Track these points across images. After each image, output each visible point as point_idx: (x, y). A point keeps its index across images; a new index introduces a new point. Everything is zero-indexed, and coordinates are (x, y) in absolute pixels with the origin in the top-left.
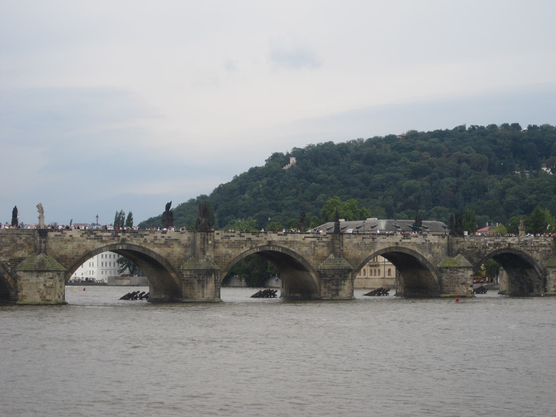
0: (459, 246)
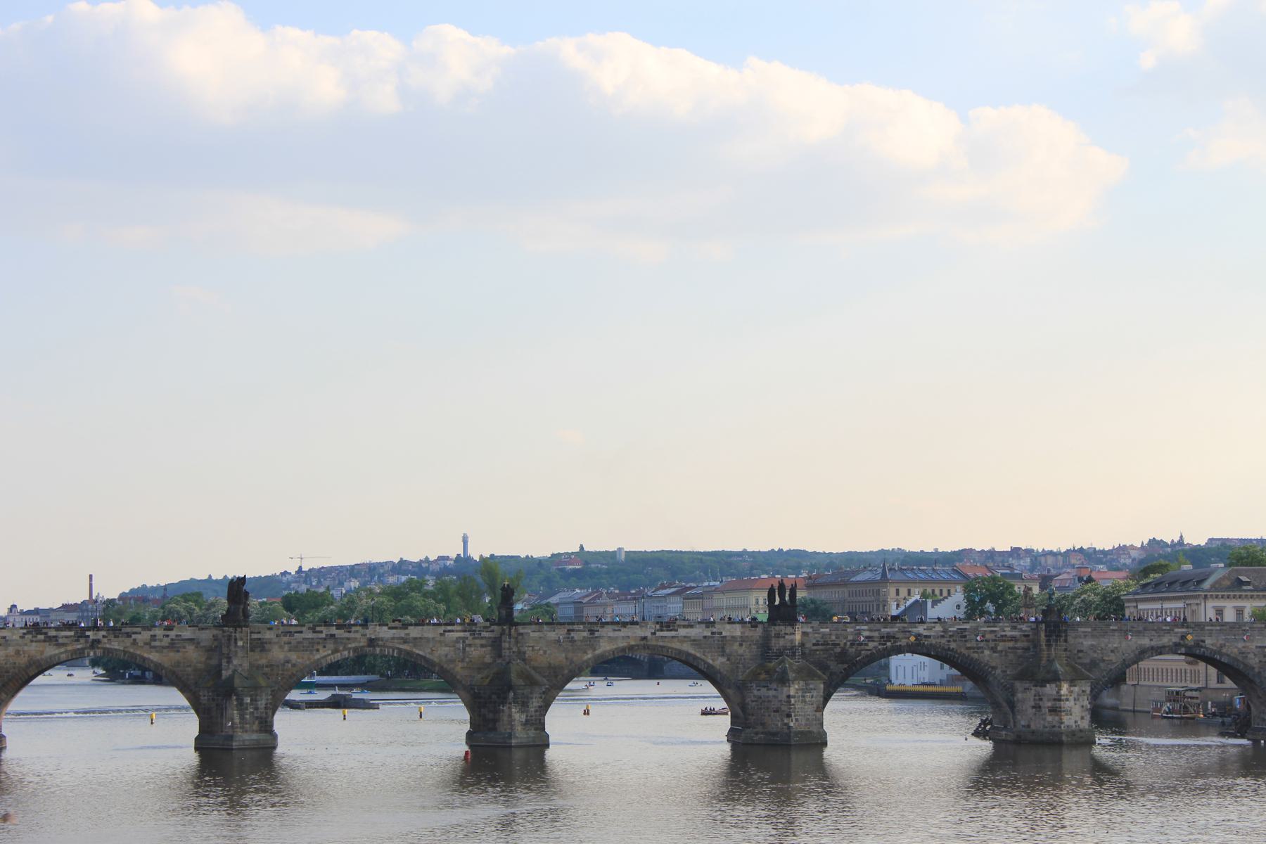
0: (782, 642)
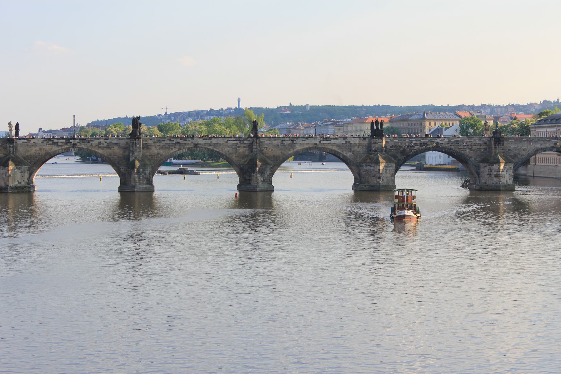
0: (377, 146)
